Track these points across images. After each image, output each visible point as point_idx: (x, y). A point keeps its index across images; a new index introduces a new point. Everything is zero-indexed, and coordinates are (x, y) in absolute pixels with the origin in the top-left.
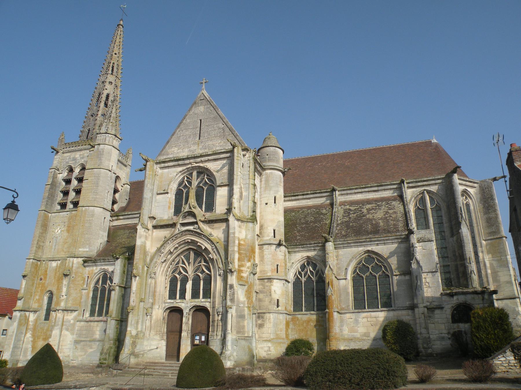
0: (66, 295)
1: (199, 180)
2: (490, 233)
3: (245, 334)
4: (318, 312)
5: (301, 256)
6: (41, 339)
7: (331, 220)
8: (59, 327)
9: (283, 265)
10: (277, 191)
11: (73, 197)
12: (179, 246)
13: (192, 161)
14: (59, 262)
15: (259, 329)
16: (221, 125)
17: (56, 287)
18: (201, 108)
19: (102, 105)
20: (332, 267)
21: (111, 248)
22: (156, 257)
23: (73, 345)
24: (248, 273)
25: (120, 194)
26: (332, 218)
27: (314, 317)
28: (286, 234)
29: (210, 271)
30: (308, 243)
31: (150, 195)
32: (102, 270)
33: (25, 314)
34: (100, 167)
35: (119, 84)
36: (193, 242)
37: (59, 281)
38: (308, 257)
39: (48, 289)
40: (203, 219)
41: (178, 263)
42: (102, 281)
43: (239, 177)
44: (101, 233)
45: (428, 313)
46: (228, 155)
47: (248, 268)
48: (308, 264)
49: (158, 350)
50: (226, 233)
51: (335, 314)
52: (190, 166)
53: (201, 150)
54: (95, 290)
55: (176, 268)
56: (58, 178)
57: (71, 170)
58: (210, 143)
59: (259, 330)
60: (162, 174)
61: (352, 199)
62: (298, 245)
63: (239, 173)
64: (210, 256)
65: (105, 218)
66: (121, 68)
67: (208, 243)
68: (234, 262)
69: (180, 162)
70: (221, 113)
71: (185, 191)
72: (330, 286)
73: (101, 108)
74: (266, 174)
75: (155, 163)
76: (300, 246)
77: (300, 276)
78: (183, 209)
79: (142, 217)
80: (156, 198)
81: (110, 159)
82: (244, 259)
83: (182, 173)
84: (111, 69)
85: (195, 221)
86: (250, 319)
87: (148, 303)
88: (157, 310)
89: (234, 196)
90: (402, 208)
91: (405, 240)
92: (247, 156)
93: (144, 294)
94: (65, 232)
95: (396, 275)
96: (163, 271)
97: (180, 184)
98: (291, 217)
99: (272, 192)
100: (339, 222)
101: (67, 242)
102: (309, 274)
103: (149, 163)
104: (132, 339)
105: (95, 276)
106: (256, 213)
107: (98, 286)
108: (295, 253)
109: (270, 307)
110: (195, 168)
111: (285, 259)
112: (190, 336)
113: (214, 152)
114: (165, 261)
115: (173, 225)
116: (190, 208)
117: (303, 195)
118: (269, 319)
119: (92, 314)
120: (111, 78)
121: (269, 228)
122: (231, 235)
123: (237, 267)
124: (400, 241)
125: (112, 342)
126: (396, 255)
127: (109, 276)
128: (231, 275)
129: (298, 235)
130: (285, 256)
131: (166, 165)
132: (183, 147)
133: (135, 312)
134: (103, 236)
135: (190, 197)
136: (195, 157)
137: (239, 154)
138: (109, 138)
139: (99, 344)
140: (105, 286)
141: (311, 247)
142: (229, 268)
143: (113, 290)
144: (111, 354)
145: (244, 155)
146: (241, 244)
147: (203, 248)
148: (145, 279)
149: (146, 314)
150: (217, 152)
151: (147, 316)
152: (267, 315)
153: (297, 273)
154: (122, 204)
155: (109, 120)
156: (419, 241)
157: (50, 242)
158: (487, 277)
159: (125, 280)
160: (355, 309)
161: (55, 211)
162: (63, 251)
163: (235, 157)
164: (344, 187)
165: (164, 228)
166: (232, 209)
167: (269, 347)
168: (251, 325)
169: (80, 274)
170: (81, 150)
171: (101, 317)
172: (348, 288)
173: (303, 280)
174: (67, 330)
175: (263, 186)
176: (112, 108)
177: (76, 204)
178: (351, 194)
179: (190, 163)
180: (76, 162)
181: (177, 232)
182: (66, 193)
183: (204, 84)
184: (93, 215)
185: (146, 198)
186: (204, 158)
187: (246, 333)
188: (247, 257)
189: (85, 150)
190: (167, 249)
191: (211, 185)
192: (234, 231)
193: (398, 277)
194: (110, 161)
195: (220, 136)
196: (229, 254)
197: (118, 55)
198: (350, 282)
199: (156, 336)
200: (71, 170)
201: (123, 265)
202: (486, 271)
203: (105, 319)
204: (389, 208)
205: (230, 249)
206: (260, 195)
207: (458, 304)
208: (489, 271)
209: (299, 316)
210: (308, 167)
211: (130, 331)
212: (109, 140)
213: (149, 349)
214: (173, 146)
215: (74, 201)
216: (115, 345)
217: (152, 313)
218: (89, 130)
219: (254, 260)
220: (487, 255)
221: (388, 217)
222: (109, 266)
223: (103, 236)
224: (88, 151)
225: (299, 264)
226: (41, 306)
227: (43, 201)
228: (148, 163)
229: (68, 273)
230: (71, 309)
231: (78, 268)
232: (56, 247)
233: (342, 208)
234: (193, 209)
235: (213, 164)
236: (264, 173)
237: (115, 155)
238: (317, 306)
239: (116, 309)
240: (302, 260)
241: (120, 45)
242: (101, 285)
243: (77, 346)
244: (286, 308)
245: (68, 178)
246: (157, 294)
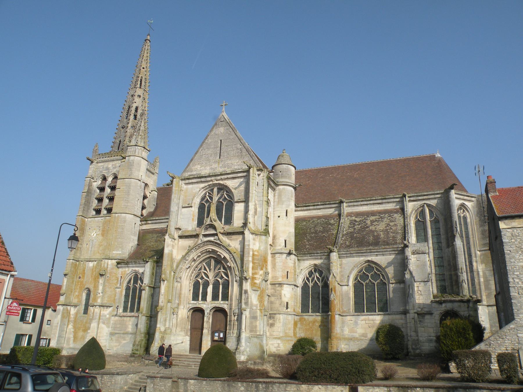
0: (102, 293)
1: (219, 195)
2: (484, 244)
3: (257, 333)
4: (322, 314)
5: (309, 263)
6: (81, 331)
7: (338, 230)
8: (97, 320)
9: (293, 271)
10: (288, 206)
11: (107, 204)
12: (202, 254)
13: (213, 178)
14: (95, 263)
15: (270, 327)
16: (239, 146)
17: (93, 285)
18: (221, 130)
19: (132, 117)
20: (335, 275)
21: (141, 251)
22: (181, 263)
23: (109, 337)
24: (260, 280)
25: (148, 200)
26: (338, 228)
27: (319, 318)
28: (296, 243)
29: (228, 277)
30: (315, 252)
31: (176, 208)
33: (67, 308)
35: (147, 97)
36: (214, 251)
37: (96, 280)
38: (315, 265)
39: (86, 287)
40: (222, 231)
41: (200, 269)
42: (133, 281)
43: (254, 195)
44: (132, 237)
45: (418, 318)
46: (245, 174)
47: (261, 275)
48: (315, 271)
49: (183, 344)
50: (242, 244)
51: (337, 317)
52: (211, 183)
53: (221, 168)
54: (128, 288)
56: (93, 186)
57: (105, 179)
58: (229, 162)
59: (271, 329)
60: (187, 189)
63: (254, 192)
64: (228, 264)
66: (148, 81)
67: (227, 253)
68: (248, 271)
69: (203, 179)
70: (239, 134)
71: (207, 205)
72: (333, 292)
73: (131, 120)
74: (279, 189)
76: (308, 255)
77: (308, 281)
78: (205, 222)
79: (170, 228)
80: (181, 210)
81: (139, 170)
82: (257, 268)
84: (139, 83)
85: (216, 233)
87: (175, 303)
88: (182, 310)
89: (249, 212)
90: (402, 220)
92: (262, 175)
93: (171, 296)
94: (100, 235)
95: (392, 283)
97: (203, 199)
98: (302, 225)
99: (284, 206)
100: (345, 232)
101: (102, 245)
102: (316, 280)
105: (127, 276)
106: (268, 227)
107: (130, 285)
108: (303, 261)
109: (280, 309)
111: (295, 267)
112: (210, 333)
113: (233, 172)
114: (189, 267)
115: (196, 236)
116: (211, 221)
117: (314, 206)
118: (279, 319)
119: (125, 310)
120: (139, 92)
121: (281, 239)
122: (246, 247)
123: (251, 275)
124: (396, 253)
125: (143, 335)
126: (393, 265)
127: (139, 277)
128: (246, 282)
129: (307, 244)
130: (295, 263)
131: (190, 181)
133: (164, 311)
134: (134, 240)
135: (211, 212)
136: (215, 176)
137: (254, 174)
138: (139, 150)
140: (137, 286)
142: (244, 276)
143: (144, 290)
144: (142, 346)
145: (259, 175)
146: (255, 254)
147: (223, 257)
148: (172, 282)
149: (173, 313)
150: (235, 171)
151: (174, 315)
152: (278, 316)
153: (306, 279)
154: (150, 209)
156: (413, 253)
157: (87, 244)
158: (480, 285)
159: (154, 280)
160: (355, 312)
161: (91, 216)
162: (99, 252)
163: (250, 177)
166: (247, 224)
167: (279, 344)
168: (262, 325)
169: (114, 274)
170: (113, 161)
171: (133, 313)
172: (350, 293)
173: (311, 285)
174: (104, 323)
175: (276, 200)
176: (141, 122)
177: (109, 210)
179: (212, 181)
180: (109, 172)
181: (200, 242)
182: (100, 200)
183: (224, 106)
184: (125, 222)
185: (173, 212)
186: (223, 176)
187: (258, 332)
188: (259, 266)
189: (117, 160)
190: (191, 257)
191: (229, 201)
193: (394, 285)
196: (245, 264)
197: (145, 69)
198: (351, 288)
200: (105, 179)
201: (152, 267)
202: (479, 280)
203: (136, 314)
204: (391, 220)
205: (245, 259)
206: (274, 208)
207: (446, 311)
208: (482, 280)
209: (306, 317)
210: (320, 178)
211: (160, 327)
212: (139, 152)
213: (175, 343)
214: (196, 164)
215: (108, 207)
217: (178, 312)
218: (120, 142)
219: (267, 269)
220: (480, 265)
221: (389, 229)
222: (140, 267)
223: (134, 240)
224: (120, 162)
225: (307, 271)
226: (80, 301)
227: (81, 207)
228: (174, 179)
229: (104, 274)
230: (107, 305)
231: (112, 269)
232: (93, 249)
233: (348, 219)
234: (213, 222)
235: (232, 182)
236: (277, 188)
237: (144, 165)
238: (322, 308)
239: (147, 306)
241: (147, 60)
243: (113, 338)
244: (294, 310)
245: (102, 186)
246: (182, 296)
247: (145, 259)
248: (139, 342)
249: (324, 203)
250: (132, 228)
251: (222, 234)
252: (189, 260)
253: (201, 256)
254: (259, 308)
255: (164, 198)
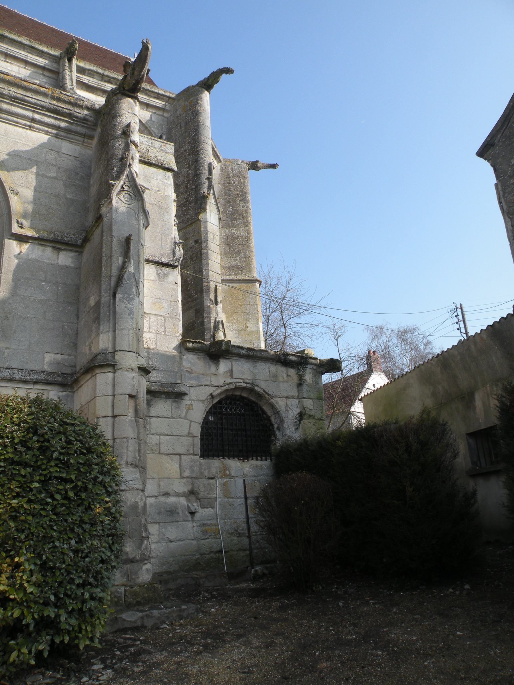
2: (229, 268)
91: (84, 131)
95: (21, 239)
124: (63, 125)
126: (34, 169)
193: (25, 247)
207: (227, 390)
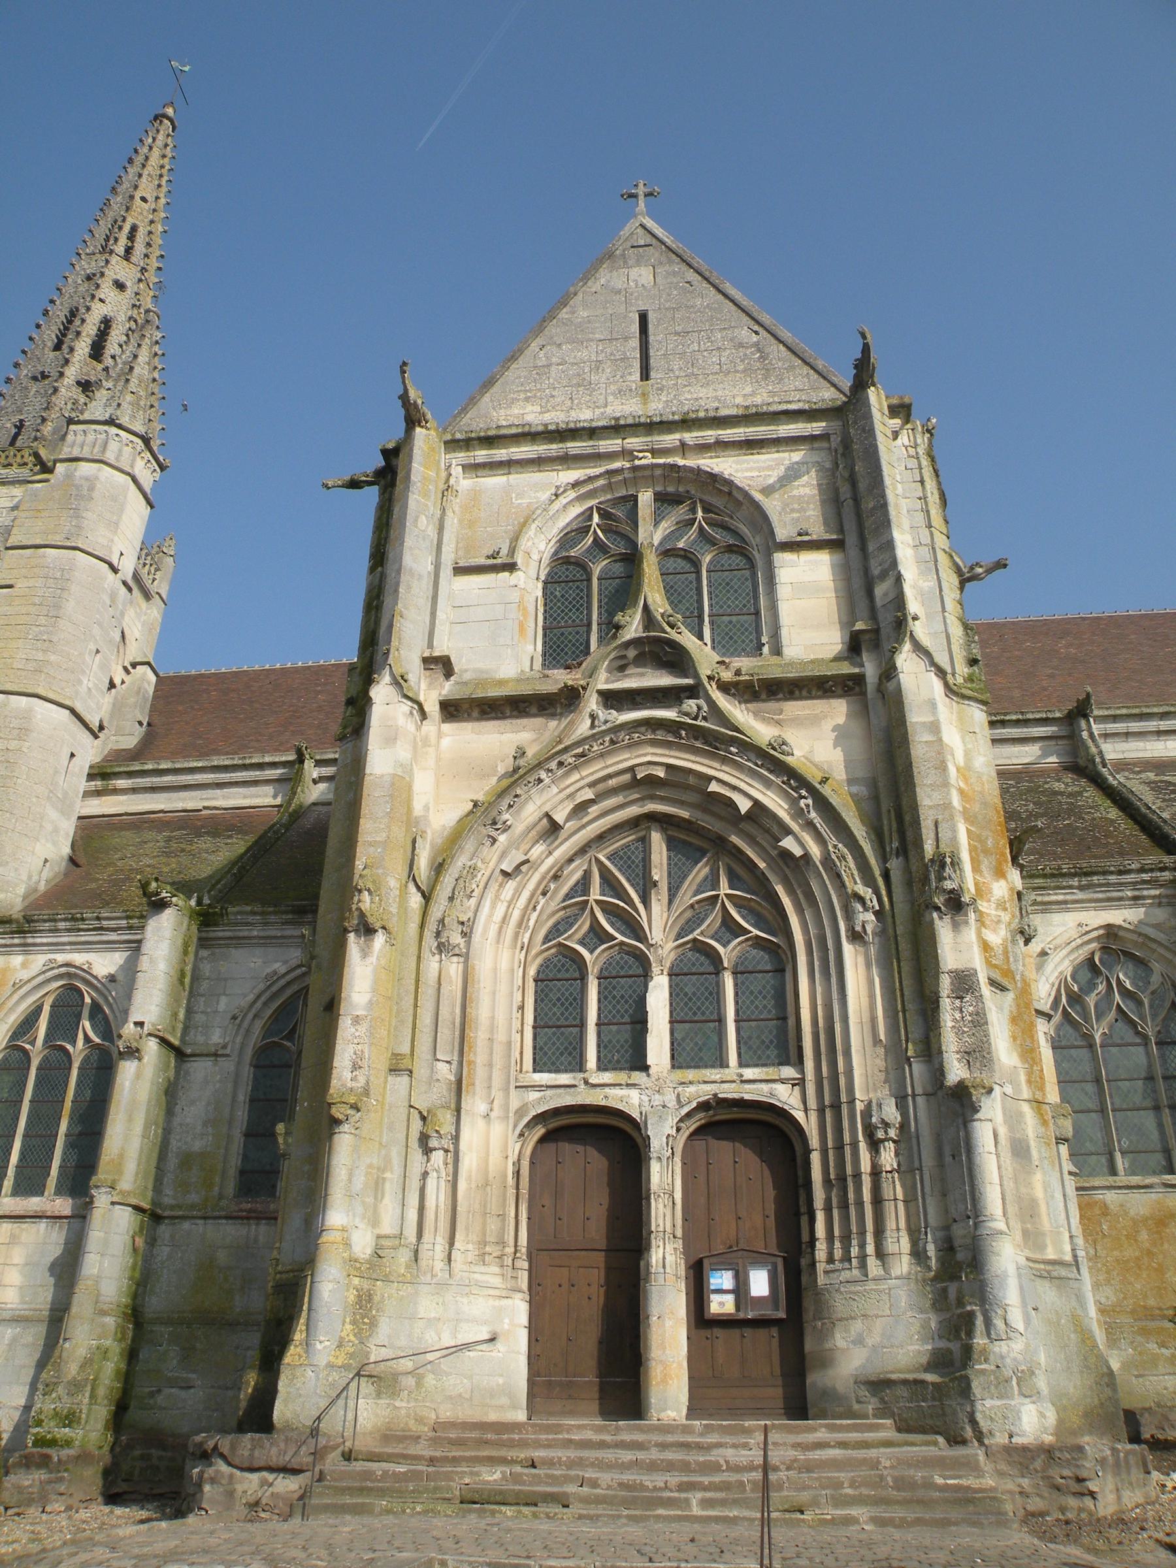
3: (1042, 1247)
13: (633, 442)
16: (745, 334)
19: (83, 347)
21: (94, 885)
22: (469, 846)
25: (116, 698)
32: (56, 971)
34: (73, 544)
38: (1111, 931)
41: (583, 885)
42: (50, 1022)
44: (53, 814)
47: (1001, 905)
55: (569, 911)
60: (475, 495)
61: (1148, 755)
62: (1063, 875)
65: (72, 755)
66: (158, 253)
69: (575, 447)
75: (446, 443)
76: (1075, 882)
81: (117, 524)
83: (583, 490)
86: (1053, 1166)
87: (432, 1080)
88: (481, 1123)
96: (505, 919)
103: (424, 430)
104: (356, 1281)
105: (16, 997)
107: (28, 1046)
110: (647, 473)
125: (110, 1321)
127: (88, 1000)
128: (956, 926)
132: (569, 403)
134: (56, 830)
138: (122, 447)
139: (14, 1340)
140: (69, 1047)
141: (1121, 884)
142: (948, 885)
143: (133, 1053)
153: (1064, 1000)
155: (122, 383)
159: (182, 1015)
164: (1119, 708)
165: (504, 718)
171: (35, 1200)
178: (1141, 735)
181: (583, 728)
183: (641, 198)
184: (23, 732)
186: (695, 434)
192: (932, 719)
194: (115, 532)
195: (744, 371)
199: (483, 1269)
201: (180, 942)
209: (1110, 1197)
212: (120, 451)
216: (120, 1341)
223: (56, 830)
225: (1067, 963)
235: (737, 463)
239: (141, 1148)
240: (1082, 945)
242: (45, 1041)
246: (479, 1037)
247: (154, 885)
248: (82, 1366)
249: (998, 718)
250: (56, 772)
251: (724, 687)
252: (519, 828)
253: (594, 810)
254: (1026, 1094)
255: (180, 708)
